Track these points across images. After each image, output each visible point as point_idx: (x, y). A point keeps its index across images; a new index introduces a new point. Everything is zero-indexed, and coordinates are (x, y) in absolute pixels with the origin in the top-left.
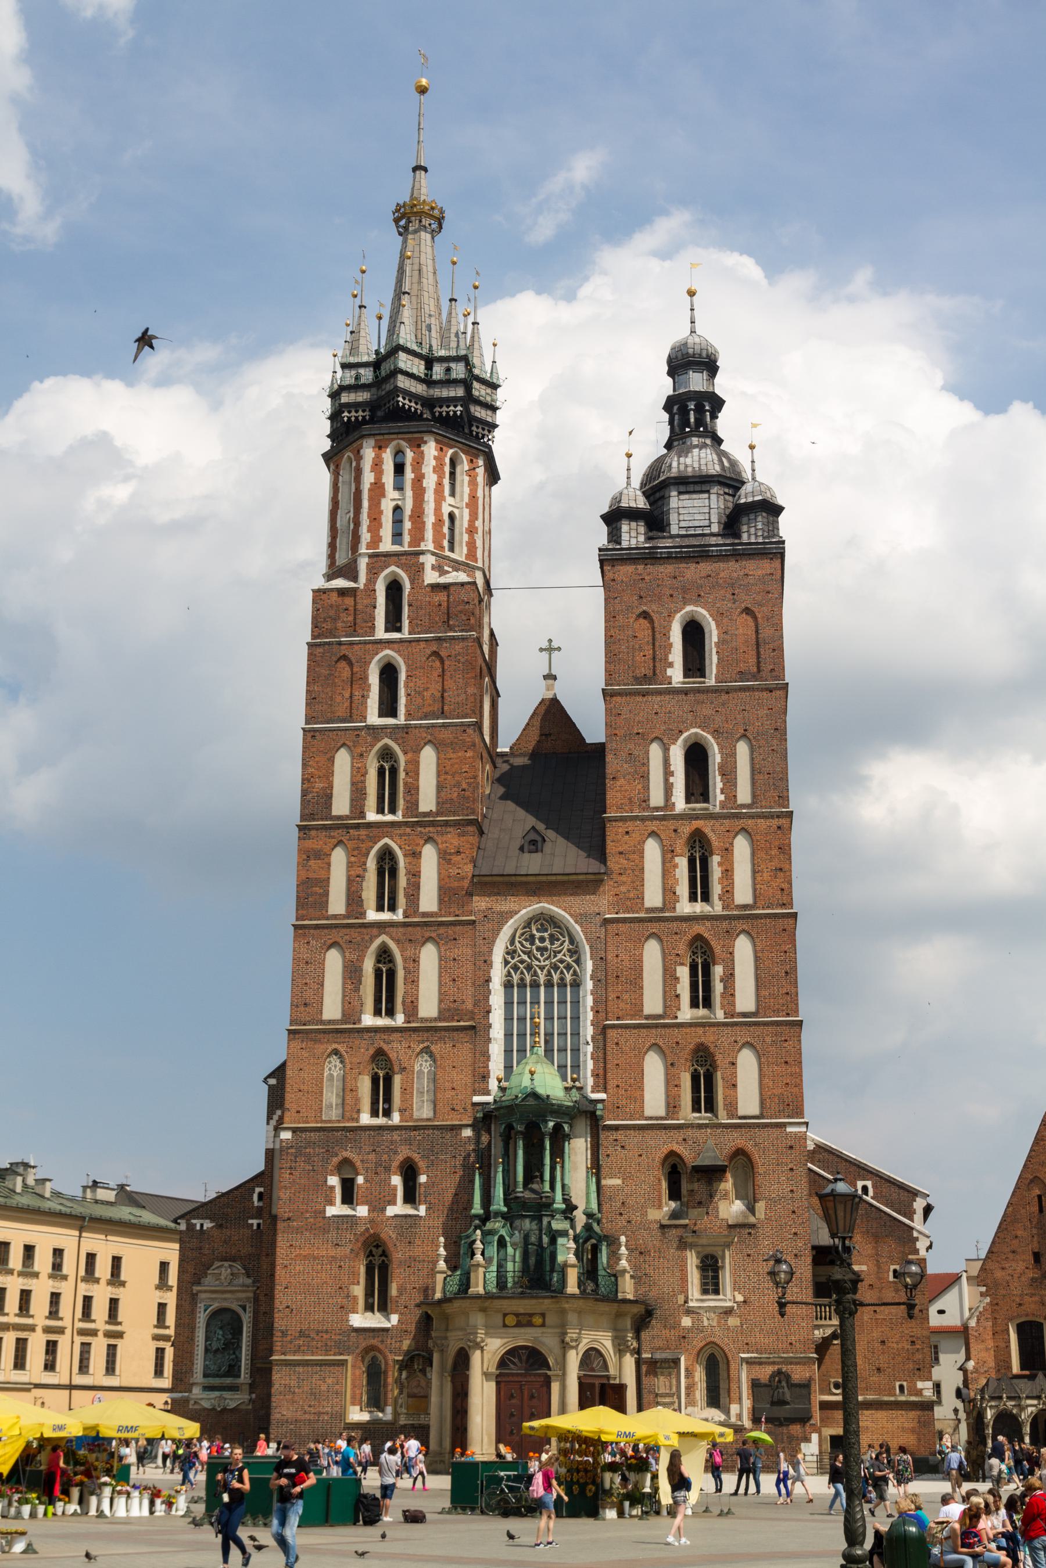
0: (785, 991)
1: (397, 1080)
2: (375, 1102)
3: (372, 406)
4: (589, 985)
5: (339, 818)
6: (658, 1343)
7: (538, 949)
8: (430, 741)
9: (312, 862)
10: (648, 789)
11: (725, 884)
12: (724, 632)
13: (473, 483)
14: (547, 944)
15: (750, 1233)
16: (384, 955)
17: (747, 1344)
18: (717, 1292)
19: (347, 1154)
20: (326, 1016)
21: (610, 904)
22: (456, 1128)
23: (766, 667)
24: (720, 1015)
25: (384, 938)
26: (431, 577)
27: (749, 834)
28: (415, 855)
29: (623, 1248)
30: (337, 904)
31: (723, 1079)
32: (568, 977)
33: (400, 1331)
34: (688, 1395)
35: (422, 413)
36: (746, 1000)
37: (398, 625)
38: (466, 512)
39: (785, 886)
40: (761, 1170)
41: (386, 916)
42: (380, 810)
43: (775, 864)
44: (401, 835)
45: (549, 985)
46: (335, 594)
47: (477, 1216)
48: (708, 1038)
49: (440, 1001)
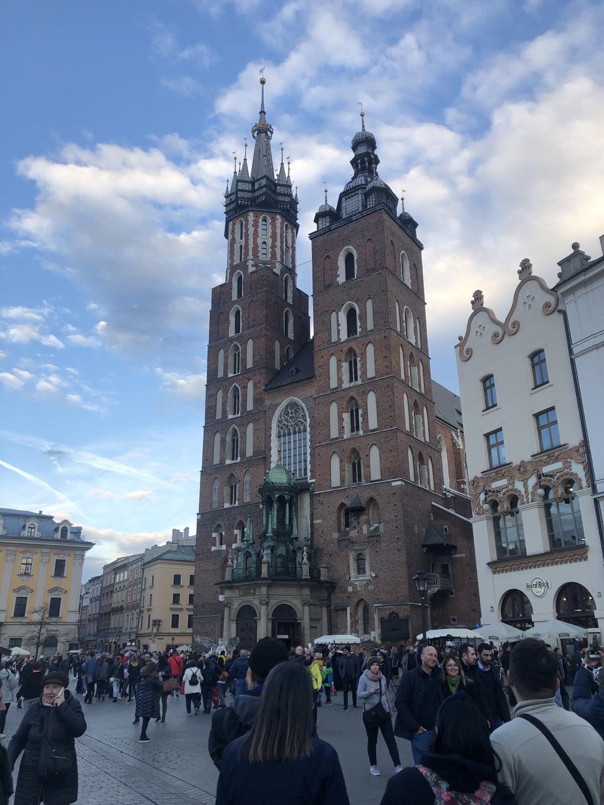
0: (388, 416)
2: (232, 497)
3: (235, 210)
4: (308, 429)
7: (291, 418)
8: (250, 338)
10: (331, 334)
11: (363, 369)
12: (359, 254)
15: (377, 540)
16: (235, 433)
17: (378, 599)
19: (219, 522)
20: (214, 464)
21: (316, 391)
22: (257, 505)
26: (251, 269)
27: (372, 343)
28: (245, 388)
29: (305, 553)
30: (219, 416)
31: (363, 463)
32: (302, 428)
34: (351, 627)
35: (251, 205)
36: (373, 423)
39: (387, 364)
42: (235, 373)
44: (240, 380)
45: (295, 433)
49: (253, 449)
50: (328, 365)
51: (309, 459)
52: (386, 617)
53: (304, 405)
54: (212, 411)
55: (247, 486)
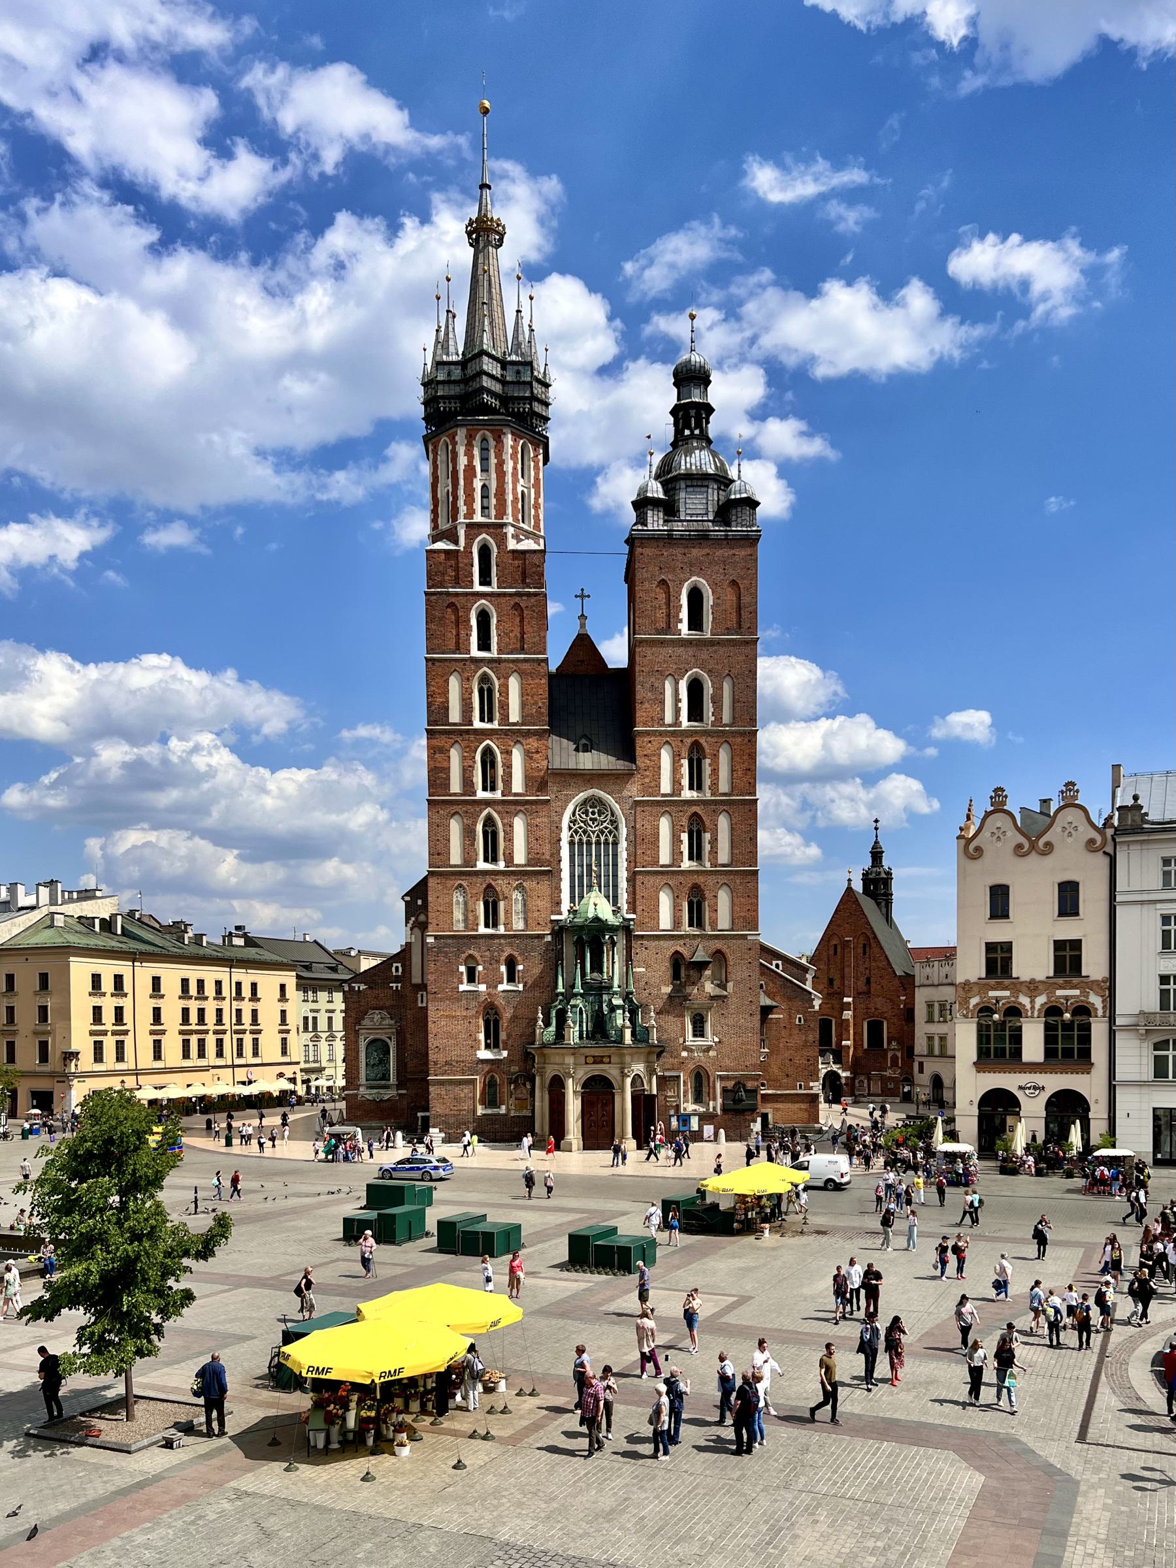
1: (502, 904)
4: (623, 845)
6: (667, 1066)
9: (437, 756)
13: (537, 467)
16: (489, 821)
18: (702, 1036)
19: (471, 952)
20: (452, 862)
22: (540, 937)
28: (508, 753)
30: (456, 786)
32: (611, 839)
33: (509, 1061)
36: (724, 856)
38: (533, 491)
39: (752, 781)
41: (487, 795)
42: (482, 720)
43: (746, 765)
45: (598, 843)
47: (562, 994)
48: (700, 880)
50: (659, 755)
51: (623, 884)
53: (617, 807)
55: (519, 907)
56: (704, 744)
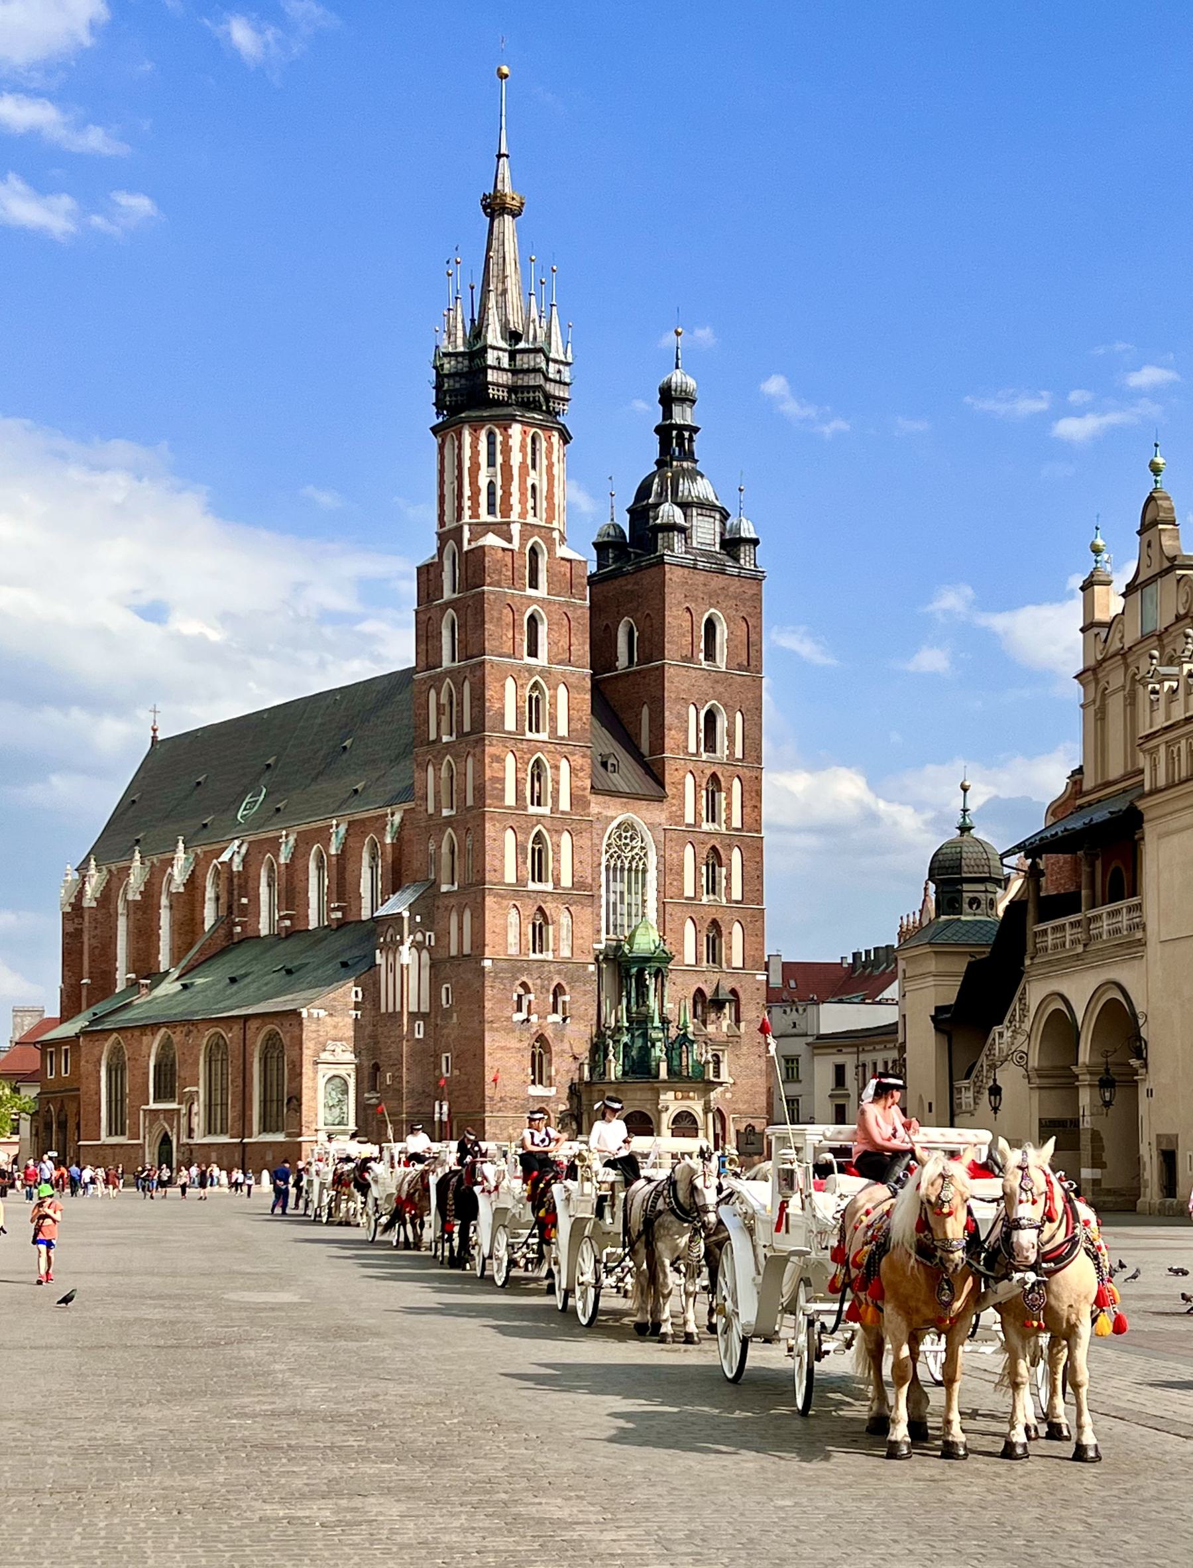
5: (510, 733)
7: (624, 844)
9: (494, 765)
12: (731, 633)
14: (628, 841)
16: (539, 837)
19: (524, 979)
23: (753, 663)
24: (724, 900)
25: (539, 827)
32: (641, 867)
37: (534, 583)
39: (758, 818)
40: (743, 1002)
43: (753, 803)
46: (500, 553)
50: (684, 784)
52: (743, 1131)
54: (497, 785)
55: (564, 933)
56: (722, 779)
